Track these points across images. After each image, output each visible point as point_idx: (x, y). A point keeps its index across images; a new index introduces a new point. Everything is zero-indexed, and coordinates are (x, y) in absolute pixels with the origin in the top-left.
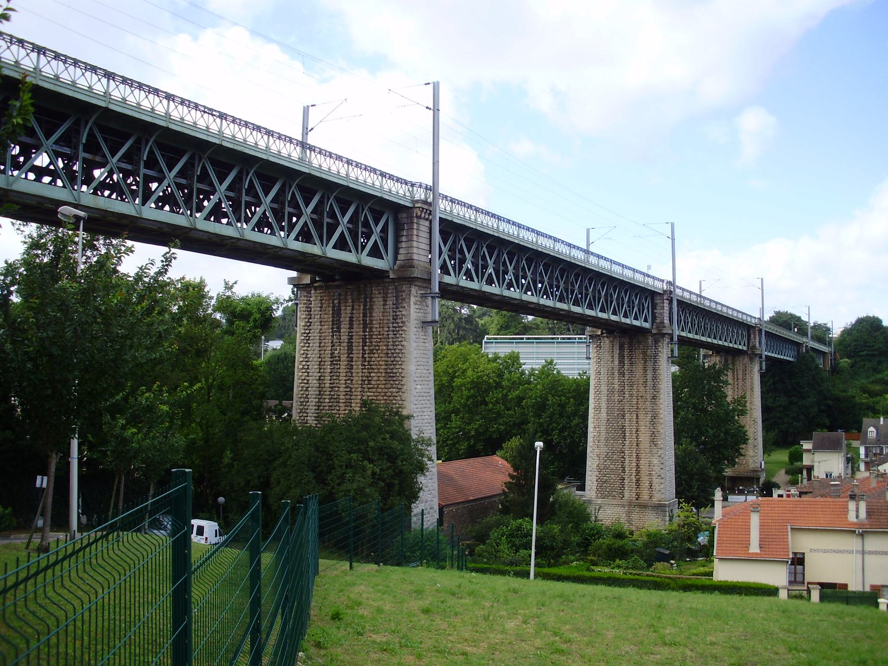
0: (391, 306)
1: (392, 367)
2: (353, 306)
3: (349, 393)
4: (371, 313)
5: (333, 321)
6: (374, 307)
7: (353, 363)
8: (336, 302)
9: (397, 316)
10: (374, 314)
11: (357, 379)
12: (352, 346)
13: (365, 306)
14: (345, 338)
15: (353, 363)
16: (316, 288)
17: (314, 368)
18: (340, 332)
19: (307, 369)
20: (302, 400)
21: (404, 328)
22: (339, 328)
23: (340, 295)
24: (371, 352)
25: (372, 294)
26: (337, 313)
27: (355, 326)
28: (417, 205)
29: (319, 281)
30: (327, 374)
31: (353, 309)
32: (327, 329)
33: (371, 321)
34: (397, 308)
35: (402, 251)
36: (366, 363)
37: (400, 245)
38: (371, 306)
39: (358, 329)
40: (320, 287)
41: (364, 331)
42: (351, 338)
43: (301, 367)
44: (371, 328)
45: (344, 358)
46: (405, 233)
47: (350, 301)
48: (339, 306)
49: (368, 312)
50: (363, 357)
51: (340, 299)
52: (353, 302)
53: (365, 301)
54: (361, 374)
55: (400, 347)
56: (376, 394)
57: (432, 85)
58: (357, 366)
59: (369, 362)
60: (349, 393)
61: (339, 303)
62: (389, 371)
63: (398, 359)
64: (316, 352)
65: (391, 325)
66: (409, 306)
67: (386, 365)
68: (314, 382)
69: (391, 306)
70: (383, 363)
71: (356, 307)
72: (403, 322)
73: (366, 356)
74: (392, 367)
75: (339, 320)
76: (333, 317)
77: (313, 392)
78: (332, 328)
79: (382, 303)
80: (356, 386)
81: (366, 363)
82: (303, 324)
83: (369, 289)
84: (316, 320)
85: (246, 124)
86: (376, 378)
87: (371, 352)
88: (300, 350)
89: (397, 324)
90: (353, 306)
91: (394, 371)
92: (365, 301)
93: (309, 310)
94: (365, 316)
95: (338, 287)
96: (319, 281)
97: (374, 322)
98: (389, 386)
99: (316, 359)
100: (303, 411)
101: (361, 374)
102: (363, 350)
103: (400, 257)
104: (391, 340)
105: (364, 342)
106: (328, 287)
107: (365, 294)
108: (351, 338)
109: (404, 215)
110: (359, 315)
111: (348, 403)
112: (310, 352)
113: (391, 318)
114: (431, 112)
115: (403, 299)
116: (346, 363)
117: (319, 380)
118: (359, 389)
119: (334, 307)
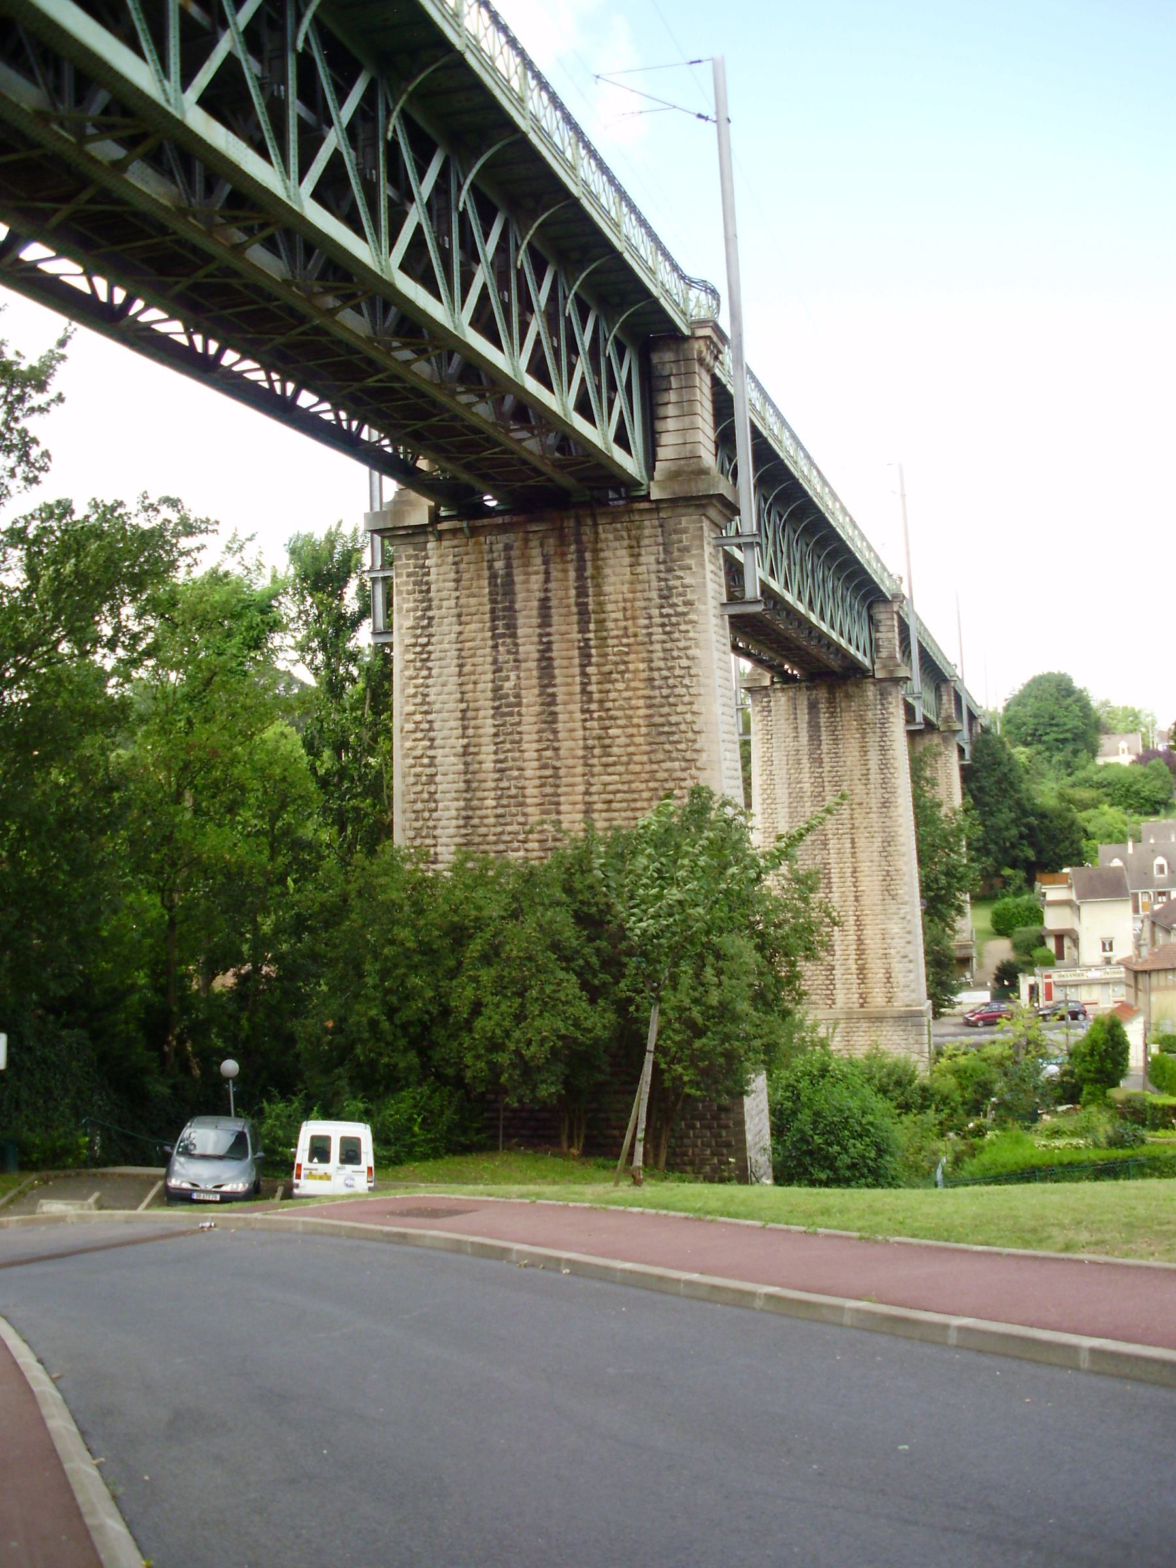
0: (654, 567)
1: (666, 710)
2: (547, 573)
3: (552, 776)
4: (598, 586)
5: (493, 611)
6: (608, 571)
7: (558, 709)
8: (499, 565)
9: (670, 588)
10: (607, 589)
11: (571, 745)
12: (550, 667)
13: (580, 570)
14: (529, 649)
15: (558, 709)
16: (440, 536)
17: (447, 728)
18: (514, 636)
19: (427, 732)
20: (419, 806)
21: (693, 617)
22: (512, 628)
23: (508, 548)
24: (606, 677)
25: (596, 540)
26: (503, 592)
27: (555, 619)
28: (700, 332)
29: (447, 518)
30: (484, 740)
31: (547, 580)
32: (478, 630)
33: (600, 604)
34: (670, 570)
35: (665, 439)
36: (594, 706)
37: (660, 426)
38: (597, 568)
39: (564, 627)
40: (454, 532)
41: (583, 630)
42: (546, 650)
43: (410, 726)
44: (601, 622)
45: (530, 696)
46: (673, 396)
47: (538, 560)
48: (509, 575)
49: (587, 583)
50: (584, 692)
51: (508, 558)
52: (546, 562)
53: (581, 560)
54: (580, 733)
55: (684, 662)
56: (626, 777)
57: (707, 67)
58: (569, 713)
59: (601, 702)
60: (552, 776)
61: (509, 566)
62: (657, 720)
63: (680, 690)
64: (451, 687)
65: (655, 612)
66: (702, 566)
67: (649, 707)
68: (448, 762)
69: (654, 567)
70: (641, 702)
71: (555, 574)
72: (687, 603)
73: (593, 688)
74: (666, 710)
75: (511, 608)
76: (493, 601)
77: (448, 784)
78: (493, 629)
79: (627, 560)
80: (570, 762)
81: (594, 706)
82: (410, 622)
83: (587, 530)
84: (444, 610)
85: (503, 29)
86: (623, 740)
87: (606, 677)
88: (406, 686)
89: (673, 612)
90: (547, 573)
91: (673, 719)
92: (581, 560)
93: (424, 589)
94: (582, 592)
95: (503, 529)
96: (447, 518)
97: (609, 607)
98: (660, 756)
99: (451, 706)
100: (425, 830)
101: (580, 733)
102: (584, 674)
103: (662, 453)
104: (658, 647)
105: (585, 655)
106: (474, 532)
107: (578, 542)
108: (546, 650)
109: (669, 356)
110: (564, 591)
111: (551, 804)
112: (432, 691)
113: (654, 595)
114: (711, 127)
115: (686, 549)
116: (537, 708)
117: (464, 754)
118: (580, 770)
119: (493, 577)
